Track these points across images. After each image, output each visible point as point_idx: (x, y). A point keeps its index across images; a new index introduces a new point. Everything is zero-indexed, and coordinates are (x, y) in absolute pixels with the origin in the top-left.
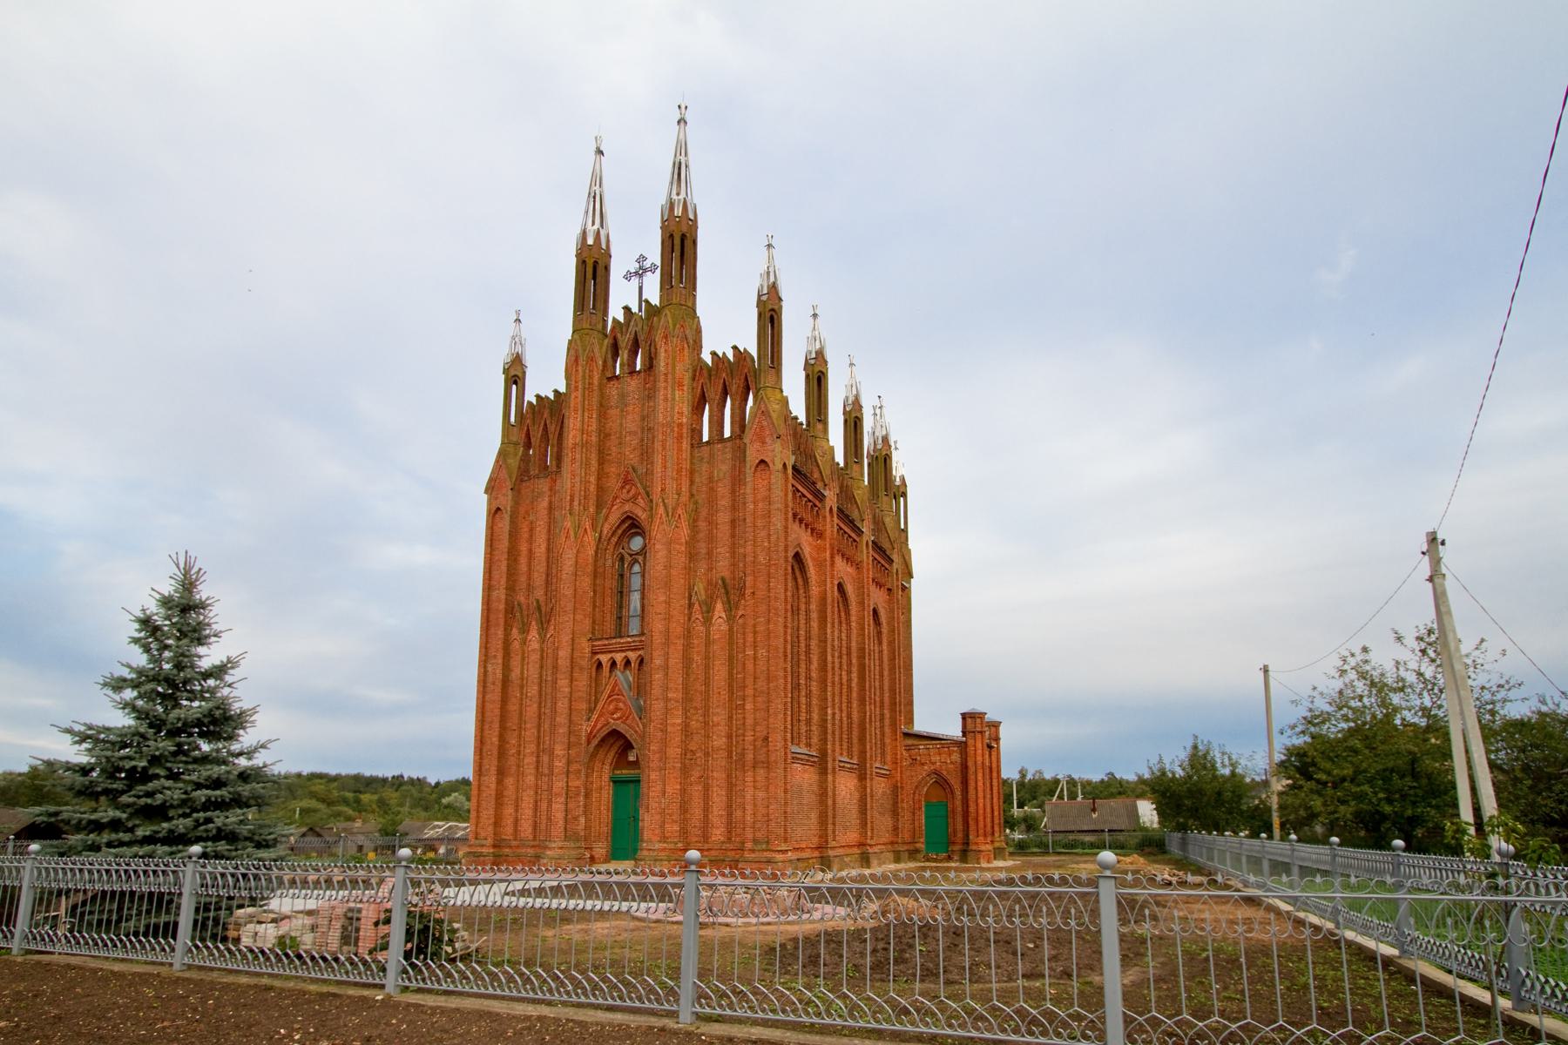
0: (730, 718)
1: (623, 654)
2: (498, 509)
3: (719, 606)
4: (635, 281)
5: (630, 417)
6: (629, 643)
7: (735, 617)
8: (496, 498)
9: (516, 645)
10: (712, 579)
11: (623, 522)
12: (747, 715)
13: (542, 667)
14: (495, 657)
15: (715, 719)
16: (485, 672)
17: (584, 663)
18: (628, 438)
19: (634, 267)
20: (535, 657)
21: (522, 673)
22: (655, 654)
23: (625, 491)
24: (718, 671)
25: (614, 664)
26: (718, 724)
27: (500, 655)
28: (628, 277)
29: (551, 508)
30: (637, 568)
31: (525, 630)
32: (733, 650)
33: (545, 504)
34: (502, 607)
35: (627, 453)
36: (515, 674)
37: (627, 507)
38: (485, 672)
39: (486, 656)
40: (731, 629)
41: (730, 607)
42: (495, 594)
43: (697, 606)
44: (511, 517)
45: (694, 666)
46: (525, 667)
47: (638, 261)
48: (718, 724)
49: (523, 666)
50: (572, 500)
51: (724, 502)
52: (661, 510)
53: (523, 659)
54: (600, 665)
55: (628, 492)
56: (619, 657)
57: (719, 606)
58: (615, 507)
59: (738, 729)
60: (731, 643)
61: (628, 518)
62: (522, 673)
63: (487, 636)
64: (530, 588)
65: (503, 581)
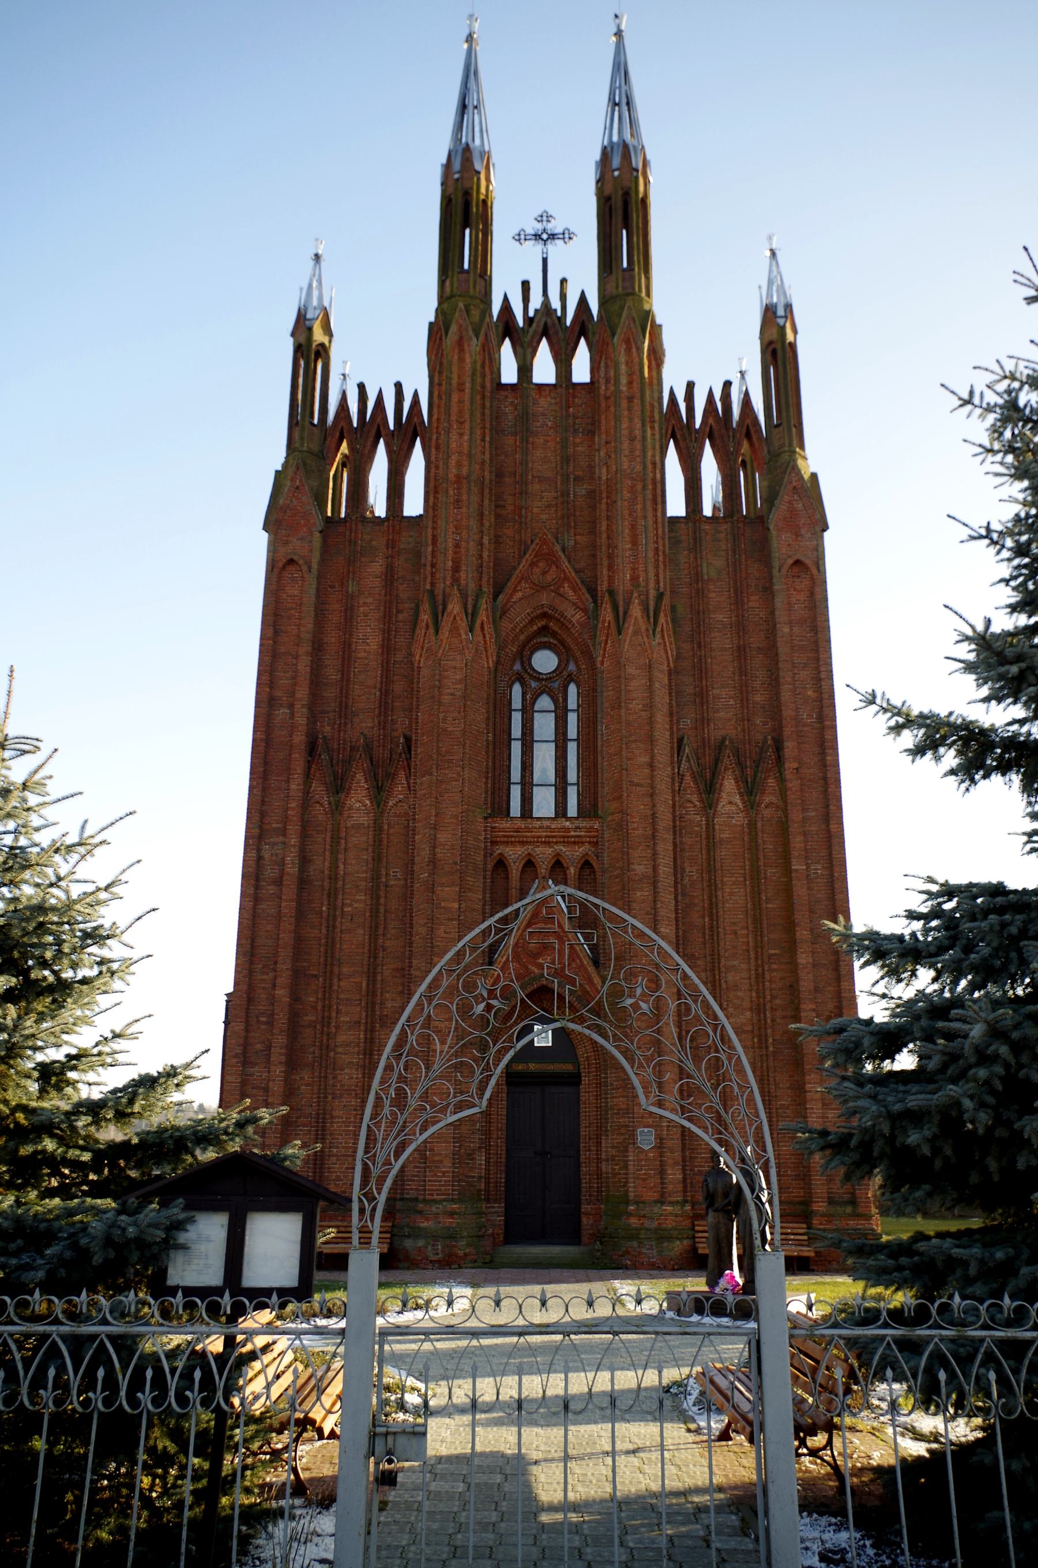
0: (760, 977)
1: (549, 851)
2: (291, 561)
3: (729, 785)
4: (534, 250)
5: (539, 453)
6: (567, 830)
7: (759, 805)
8: (286, 543)
9: (319, 813)
10: (709, 738)
11: (531, 622)
12: (802, 974)
13: (378, 859)
14: (284, 832)
15: (730, 977)
16: (260, 858)
17: (479, 858)
18: (536, 487)
19: (532, 227)
20: (359, 840)
21: (334, 866)
22: (635, 854)
23: (536, 570)
24: (731, 894)
25: (530, 864)
26: (736, 987)
27: (294, 829)
28: (520, 238)
29: (390, 578)
30: (545, 702)
31: (339, 786)
32: (758, 859)
33: (377, 567)
34: (299, 738)
35: (535, 510)
36: (320, 864)
37: (545, 599)
38: (260, 858)
39: (261, 828)
40: (752, 825)
41: (750, 790)
42: (282, 712)
43: (688, 778)
44: (319, 578)
45: (686, 880)
46: (341, 856)
47: (540, 219)
48: (736, 987)
49: (334, 853)
50: (456, 569)
51: (721, 617)
52: (636, 611)
53: (336, 840)
54: (501, 864)
55: (544, 573)
56: (544, 855)
57: (729, 785)
58: (520, 594)
59: (773, 997)
60: (754, 847)
61: (545, 615)
62: (334, 866)
63: (264, 790)
64: (345, 712)
65: (302, 693)
